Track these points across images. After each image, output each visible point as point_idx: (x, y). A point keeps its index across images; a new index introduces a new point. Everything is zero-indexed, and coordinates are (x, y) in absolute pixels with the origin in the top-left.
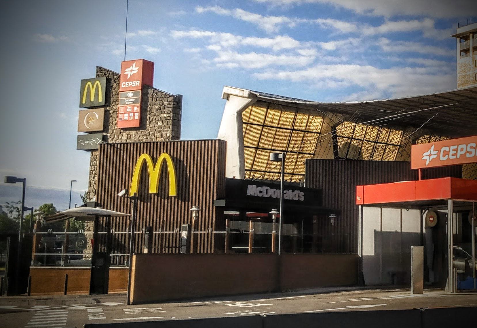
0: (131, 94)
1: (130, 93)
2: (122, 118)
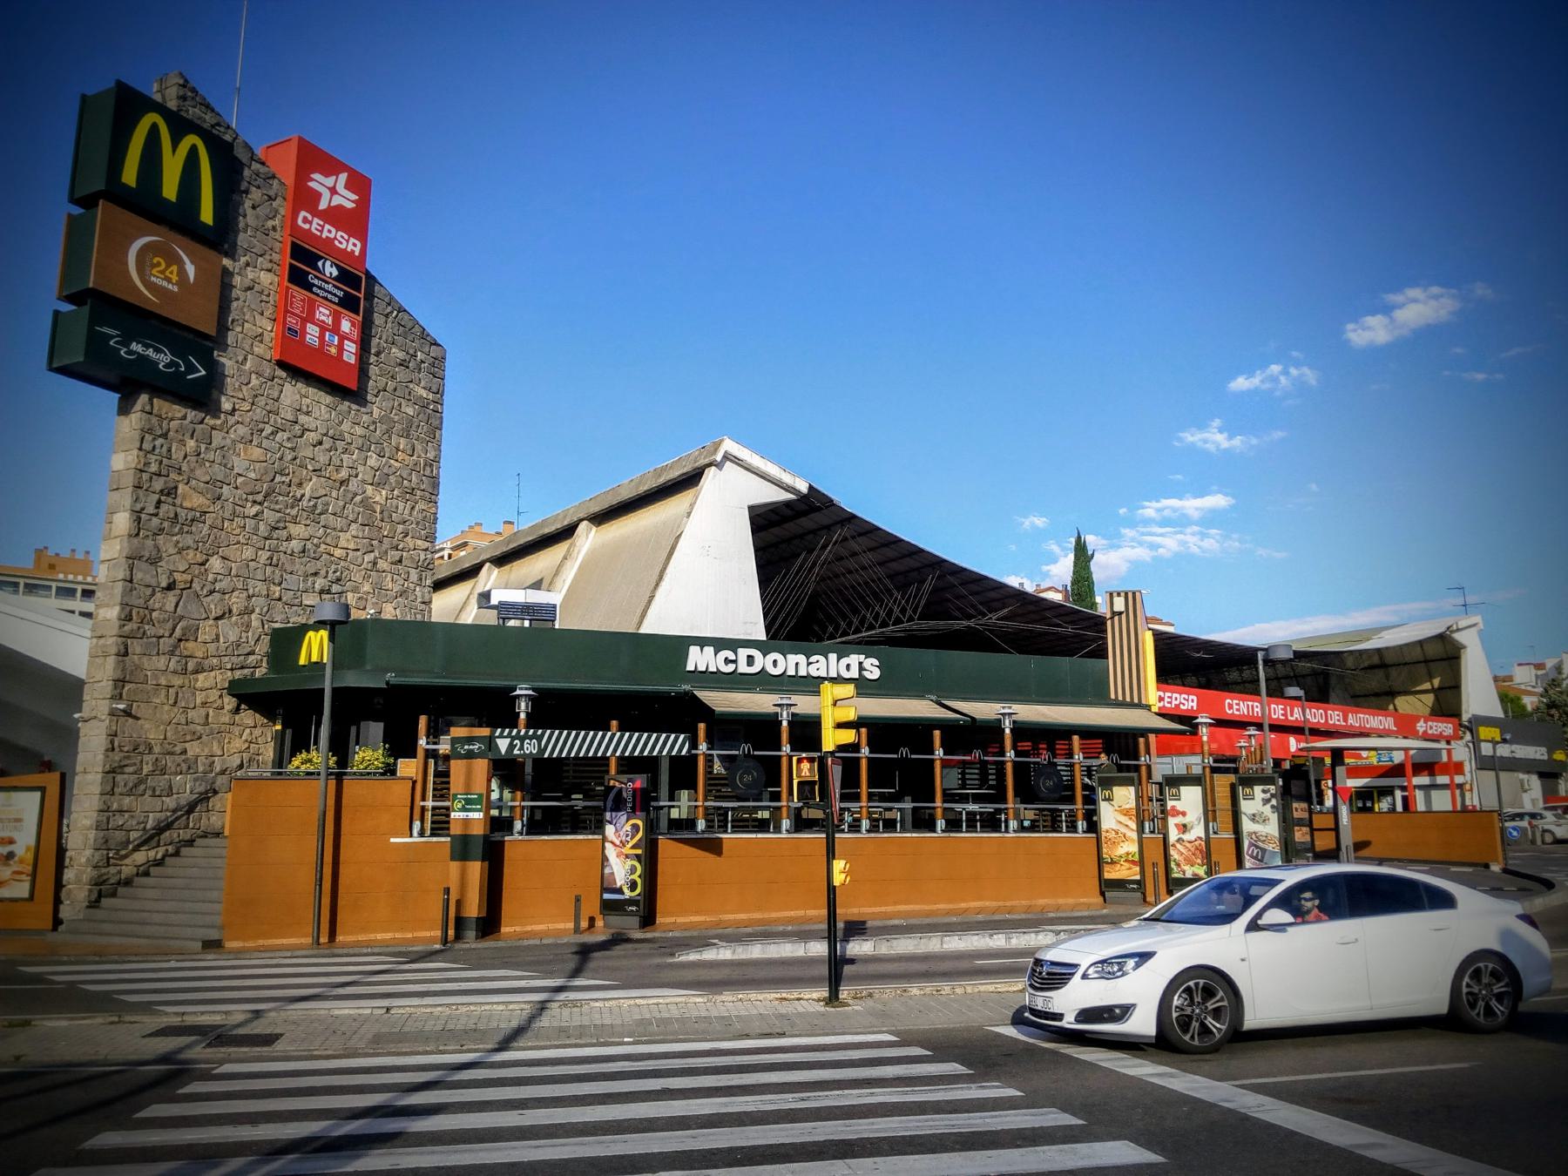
0: (331, 270)
1: (328, 263)
2: (296, 332)
